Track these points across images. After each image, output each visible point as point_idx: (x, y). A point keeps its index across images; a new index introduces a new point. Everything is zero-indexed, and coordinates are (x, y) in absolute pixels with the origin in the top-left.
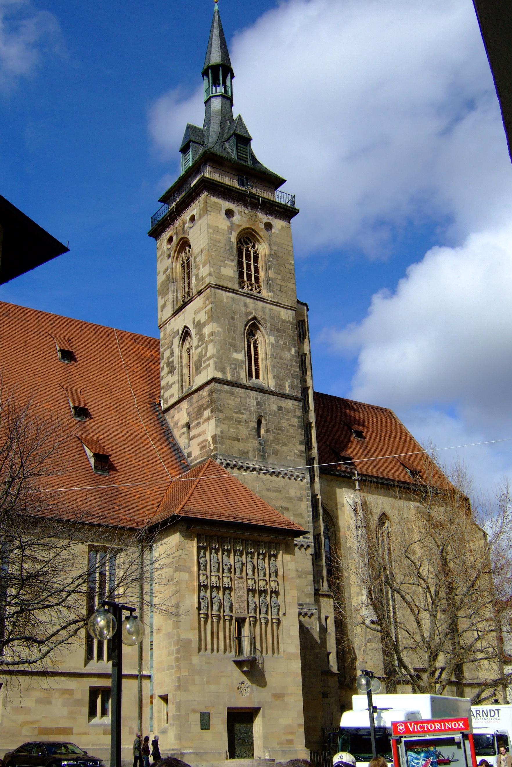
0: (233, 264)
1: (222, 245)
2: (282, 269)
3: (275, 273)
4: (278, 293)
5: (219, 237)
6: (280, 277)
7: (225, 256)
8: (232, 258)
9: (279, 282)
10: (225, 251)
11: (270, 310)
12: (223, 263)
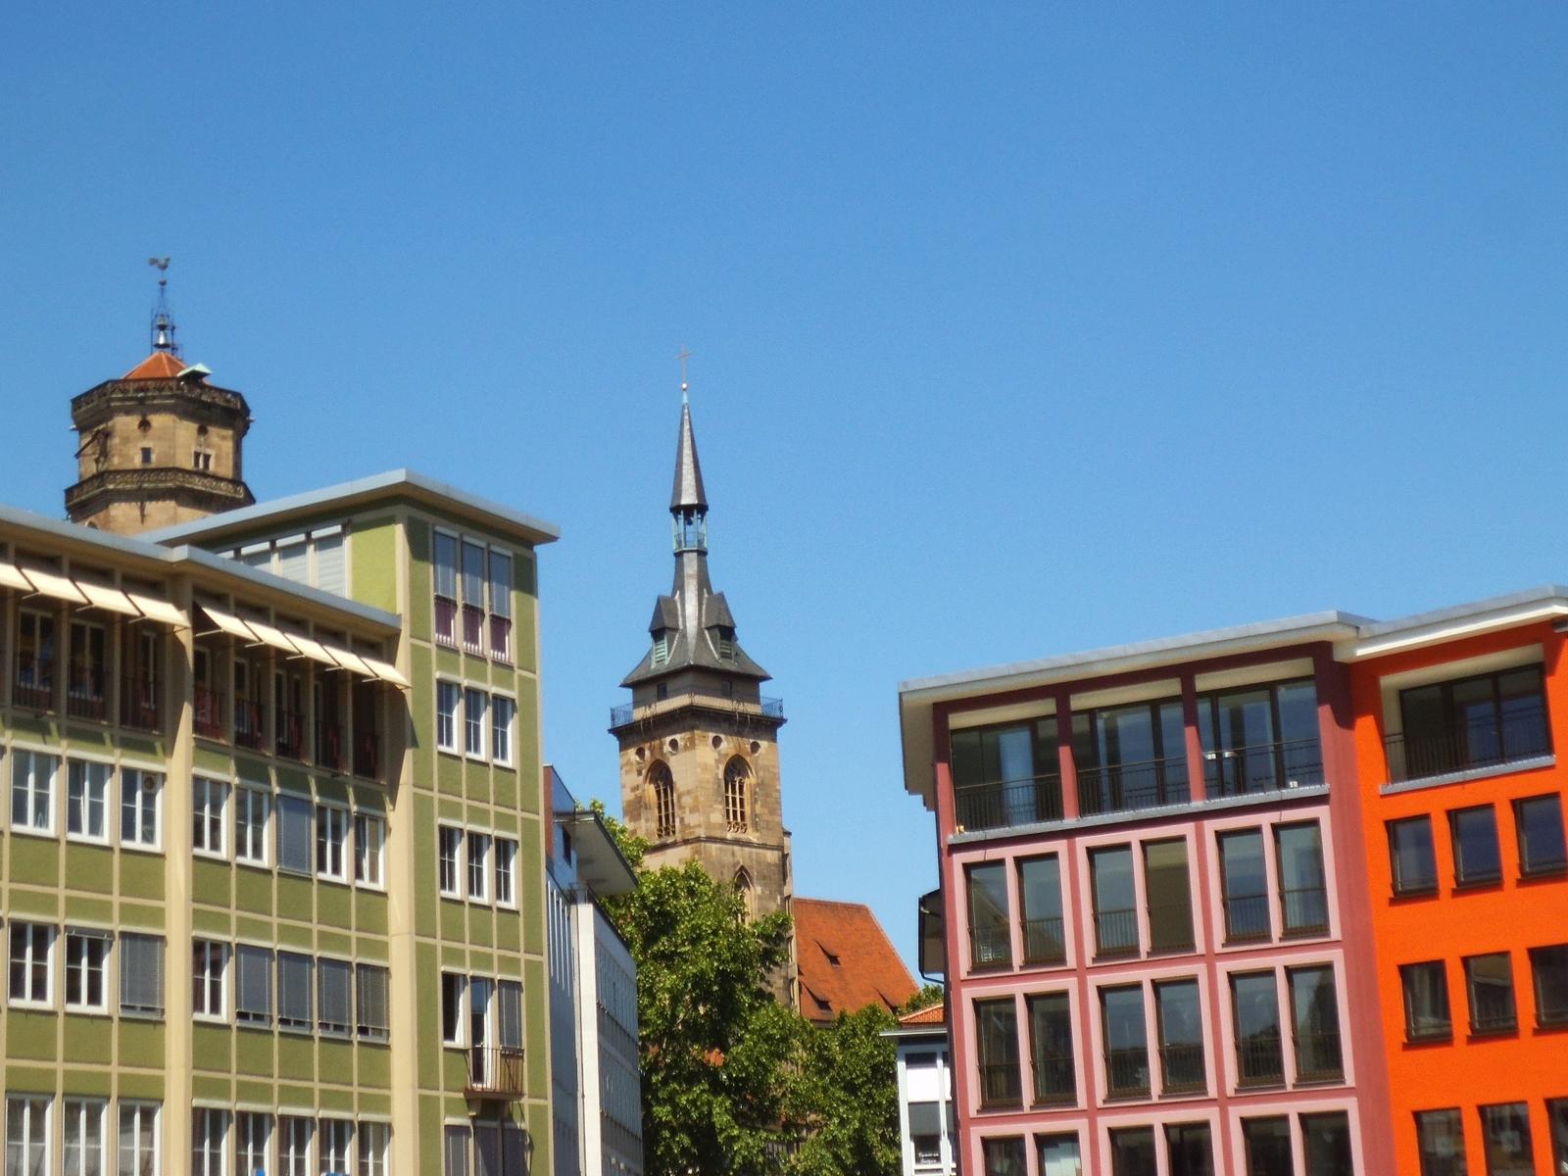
0: (721, 807)
6: (766, 811)
8: (720, 799)
9: (765, 817)
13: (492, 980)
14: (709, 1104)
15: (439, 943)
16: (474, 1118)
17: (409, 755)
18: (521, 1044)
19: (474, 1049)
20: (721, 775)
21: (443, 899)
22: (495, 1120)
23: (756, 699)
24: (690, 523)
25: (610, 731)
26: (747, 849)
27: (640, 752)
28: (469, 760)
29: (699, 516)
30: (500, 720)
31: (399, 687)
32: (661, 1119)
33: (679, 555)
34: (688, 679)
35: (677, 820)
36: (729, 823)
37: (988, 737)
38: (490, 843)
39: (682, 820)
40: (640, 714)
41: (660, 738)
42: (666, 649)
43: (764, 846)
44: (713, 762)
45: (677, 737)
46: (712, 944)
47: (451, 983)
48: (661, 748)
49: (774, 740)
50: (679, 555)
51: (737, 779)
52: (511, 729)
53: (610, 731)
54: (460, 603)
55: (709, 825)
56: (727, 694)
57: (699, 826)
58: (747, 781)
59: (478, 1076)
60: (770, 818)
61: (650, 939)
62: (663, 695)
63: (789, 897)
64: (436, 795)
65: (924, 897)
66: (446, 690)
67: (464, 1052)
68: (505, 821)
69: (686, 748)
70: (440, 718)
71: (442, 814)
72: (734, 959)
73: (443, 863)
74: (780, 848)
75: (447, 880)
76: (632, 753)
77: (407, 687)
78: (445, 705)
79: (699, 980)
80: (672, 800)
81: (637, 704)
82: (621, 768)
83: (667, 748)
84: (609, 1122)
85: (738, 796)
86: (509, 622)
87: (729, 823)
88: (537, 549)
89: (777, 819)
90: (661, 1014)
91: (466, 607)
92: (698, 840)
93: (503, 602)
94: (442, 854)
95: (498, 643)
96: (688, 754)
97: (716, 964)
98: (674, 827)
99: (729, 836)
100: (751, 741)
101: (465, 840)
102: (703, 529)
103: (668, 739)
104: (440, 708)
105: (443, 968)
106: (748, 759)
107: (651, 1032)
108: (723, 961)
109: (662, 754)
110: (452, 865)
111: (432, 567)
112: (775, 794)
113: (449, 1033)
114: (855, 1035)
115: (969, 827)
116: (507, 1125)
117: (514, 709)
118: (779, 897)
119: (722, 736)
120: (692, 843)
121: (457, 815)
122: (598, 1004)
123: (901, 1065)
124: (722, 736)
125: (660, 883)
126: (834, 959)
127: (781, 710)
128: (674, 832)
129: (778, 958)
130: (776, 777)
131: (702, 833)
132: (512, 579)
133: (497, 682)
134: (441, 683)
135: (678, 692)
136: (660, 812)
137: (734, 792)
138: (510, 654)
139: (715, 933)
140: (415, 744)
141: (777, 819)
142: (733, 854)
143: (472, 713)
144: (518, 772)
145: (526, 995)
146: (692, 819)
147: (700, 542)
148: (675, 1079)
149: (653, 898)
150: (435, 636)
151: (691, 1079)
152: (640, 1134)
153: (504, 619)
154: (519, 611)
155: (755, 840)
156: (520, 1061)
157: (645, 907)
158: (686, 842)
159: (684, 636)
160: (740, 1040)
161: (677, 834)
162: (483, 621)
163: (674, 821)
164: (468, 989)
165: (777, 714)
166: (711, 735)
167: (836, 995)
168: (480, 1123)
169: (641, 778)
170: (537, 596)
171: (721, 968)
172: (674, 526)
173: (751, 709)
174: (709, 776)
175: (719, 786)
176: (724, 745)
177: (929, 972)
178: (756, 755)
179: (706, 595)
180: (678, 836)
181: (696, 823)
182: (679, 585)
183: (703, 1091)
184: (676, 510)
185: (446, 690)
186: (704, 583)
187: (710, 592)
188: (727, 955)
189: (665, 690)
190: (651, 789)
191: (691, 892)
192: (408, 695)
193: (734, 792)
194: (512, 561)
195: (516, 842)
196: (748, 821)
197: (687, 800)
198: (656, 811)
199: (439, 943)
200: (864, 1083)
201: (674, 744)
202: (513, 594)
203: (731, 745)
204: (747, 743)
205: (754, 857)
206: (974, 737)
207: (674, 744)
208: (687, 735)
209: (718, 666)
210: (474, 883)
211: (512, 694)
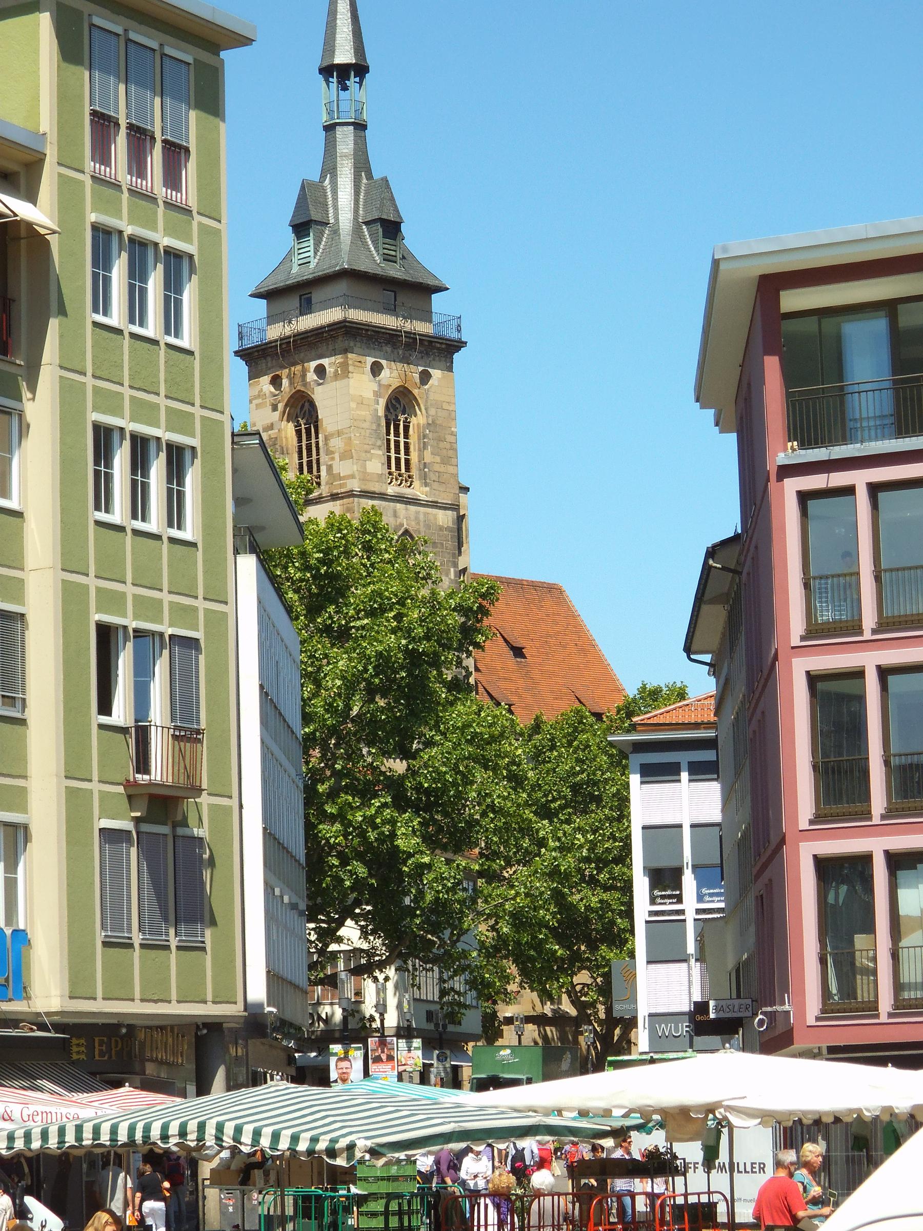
0: (380, 453)
1: (366, 425)
2: (442, 445)
3: (432, 454)
4: (435, 486)
5: (363, 413)
6: (438, 459)
7: (370, 443)
8: (379, 443)
9: (437, 467)
10: (371, 434)
11: (426, 514)
12: (368, 455)
13: (161, 635)
14: (393, 822)
15: (92, 582)
16: (137, 820)
17: (54, 325)
18: (198, 723)
19: (137, 728)
20: (381, 412)
21: (98, 523)
22: (165, 824)
23: (426, 315)
24: (345, 88)
25: (237, 353)
26: (412, 508)
27: (276, 381)
28: (133, 336)
29: (357, 79)
30: (173, 285)
31: (42, 231)
32: (327, 840)
33: (329, 129)
34: (342, 287)
35: (323, 468)
36: (390, 474)
37: (829, 324)
38: (159, 449)
39: (330, 468)
40: (276, 332)
41: (303, 362)
42: (312, 248)
43: (434, 505)
44: (370, 395)
45: (325, 362)
46: (399, 617)
47: (106, 634)
48: (304, 376)
49: (450, 369)
50: (329, 129)
51: (402, 418)
52: (189, 296)
53: (237, 353)
54: (123, 123)
55: (365, 477)
56: (391, 309)
57: (352, 476)
58: (414, 421)
59: (143, 765)
60: (442, 469)
61: (313, 610)
62: (306, 308)
63: (464, 571)
64: (89, 381)
65: (714, 547)
66: (102, 234)
67: (124, 730)
68: (179, 421)
69: (336, 376)
70: (95, 276)
71: (95, 409)
72: (427, 637)
73: (97, 473)
74: (455, 507)
75: (103, 499)
76: (265, 380)
77: (54, 232)
78: (102, 260)
79: (384, 662)
80: (317, 444)
81: (272, 319)
82: (251, 402)
83: (311, 376)
84: (271, 838)
85: (402, 439)
86: (187, 150)
87: (390, 474)
88: (223, 54)
89: (451, 469)
90: (330, 707)
91: (130, 127)
92: (350, 494)
93: (180, 124)
94: (97, 462)
95: (172, 179)
96: (339, 384)
97: (404, 642)
98: (319, 477)
99: (391, 490)
100: (421, 369)
101: (127, 444)
102: (362, 95)
103: (313, 364)
104: (95, 264)
105: (97, 617)
106: (416, 392)
107: (315, 730)
108: (414, 638)
109: (305, 384)
110: (109, 477)
111: (87, 74)
112: (450, 438)
113: (105, 707)
114: (553, 748)
115: (803, 445)
116: (180, 831)
117: (192, 270)
118: (452, 570)
119: (384, 362)
120: (342, 498)
121: (117, 411)
122: (261, 687)
123: (635, 779)
124: (384, 362)
125: (326, 535)
126: (518, 652)
127: (459, 331)
128: (319, 484)
129: (480, 638)
130: (451, 416)
131: (355, 485)
132: (192, 93)
133: (168, 232)
134: (96, 228)
135: (327, 305)
136: (300, 457)
137: (397, 434)
138: (189, 194)
139: (402, 602)
140: (62, 311)
141: (451, 469)
142: (395, 515)
143: (137, 273)
144: (197, 354)
145: (206, 657)
146: (343, 468)
147: (359, 112)
148: (347, 789)
149: (317, 555)
150: (89, 165)
151: (366, 793)
152: (303, 860)
153: (180, 147)
154: (199, 138)
155: (423, 497)
156: (199, 745)
157: (306, 567)
158: (334, 497)
159: (336, 232)
160: (429, 743)
161: (322, 487)
162: (152, 147)
163: (319, 470)
164: (130, 645)
165: (454, 335)
166: (370, 360)
167: (520, 696)
168: (146, 828)
169: (277, 414)
170: (223, 120)
171: (410, 647)
172: (326, 91)
173: (421, 328)
174: (365, 413)
175: (379, 425)
176: (385, 374)
177: (696, 653)
178: (426, 387)
179: (365, 181)
180: (324, 490)
181: (349, 473)
182: (330, 168)
183: (385, 805)
184: (327, 71)
185: (102, 234)
186: (362, 165)
187: (370, 176)
188: (420, 632)
189: (309, 301)
190: (289, 429)
191: (368, 548)
192: (53, 240)
193: (397, 434)
194: (192, 68)
195: (193, 449)
196: (414, 472)
197: (336, 444)
198: (296, 456)
199: (92, 582)
200: (562, 808)
201: (321, 371)
202: (193, 114)
203: (395, 374)
204: (414, 372)
205: (421, 517)
206: (810, 325)
207: (321, 371)
208: (339, 359)
209: (379, 271)
210: (139, 506)
211: (190, 248)
